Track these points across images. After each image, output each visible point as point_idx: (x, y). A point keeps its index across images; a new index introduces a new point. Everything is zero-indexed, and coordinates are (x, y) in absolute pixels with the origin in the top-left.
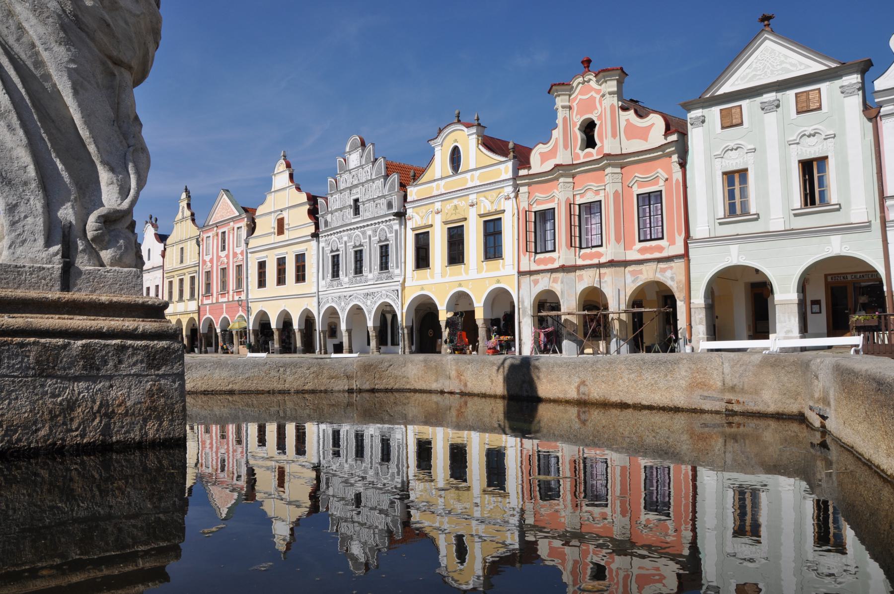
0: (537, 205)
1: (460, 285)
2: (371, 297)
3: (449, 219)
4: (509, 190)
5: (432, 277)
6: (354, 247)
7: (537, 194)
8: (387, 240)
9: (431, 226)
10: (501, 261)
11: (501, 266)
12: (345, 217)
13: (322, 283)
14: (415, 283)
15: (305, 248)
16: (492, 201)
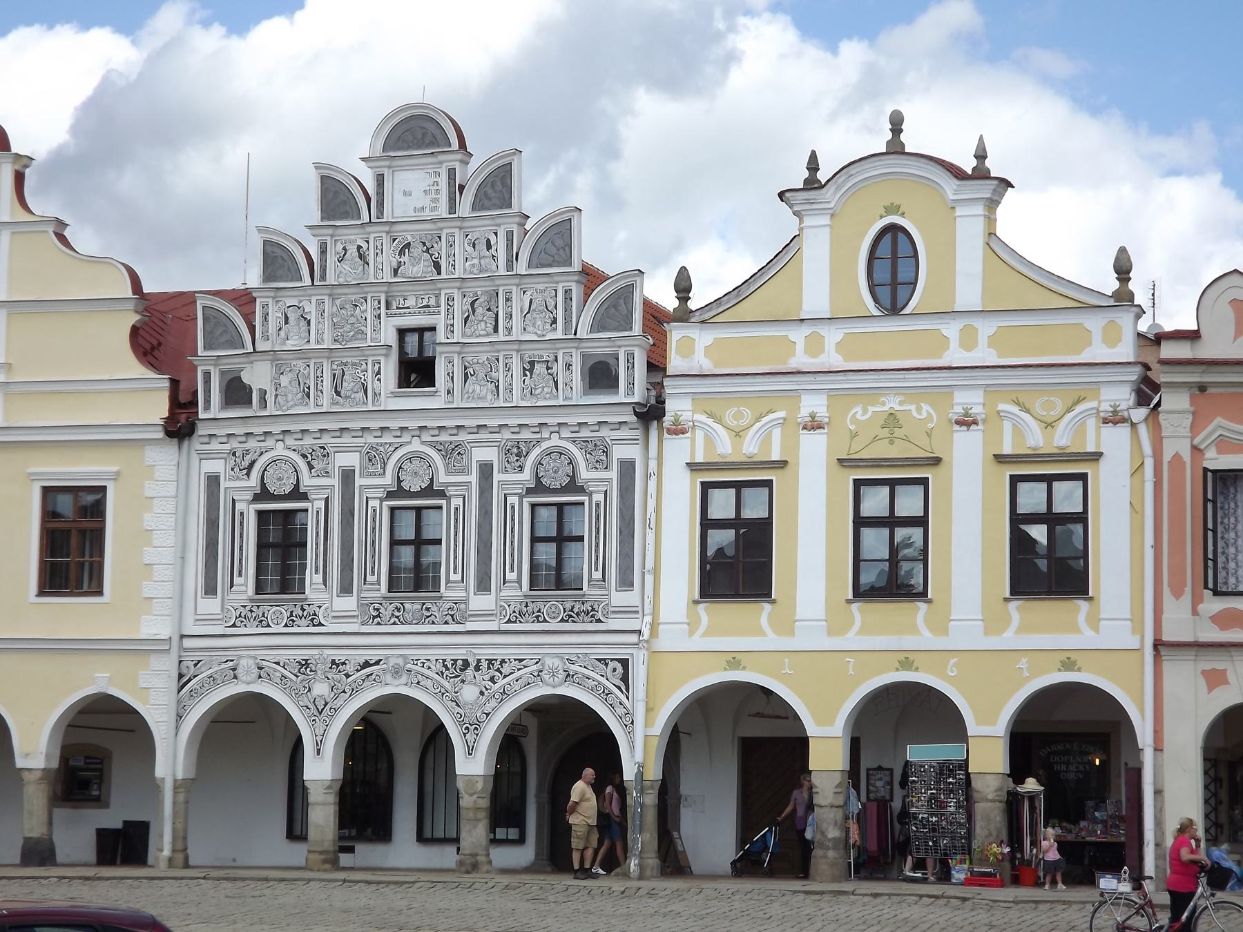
0: (1220, 452)
1: (906, 664)
2: (483, 676)
3: (865, 455)
4: (1121, 395)
5: (786, 626)
6: (390, 495)
7: (1219, 420)
8: (573, 486)
9: (782, 464)
10: (1083, 605)
11: (1081, 618)
12: (347, 386)
13: (211, 606)
14: (699, 642)
15: (115, 469)
16: (1050, 421)
